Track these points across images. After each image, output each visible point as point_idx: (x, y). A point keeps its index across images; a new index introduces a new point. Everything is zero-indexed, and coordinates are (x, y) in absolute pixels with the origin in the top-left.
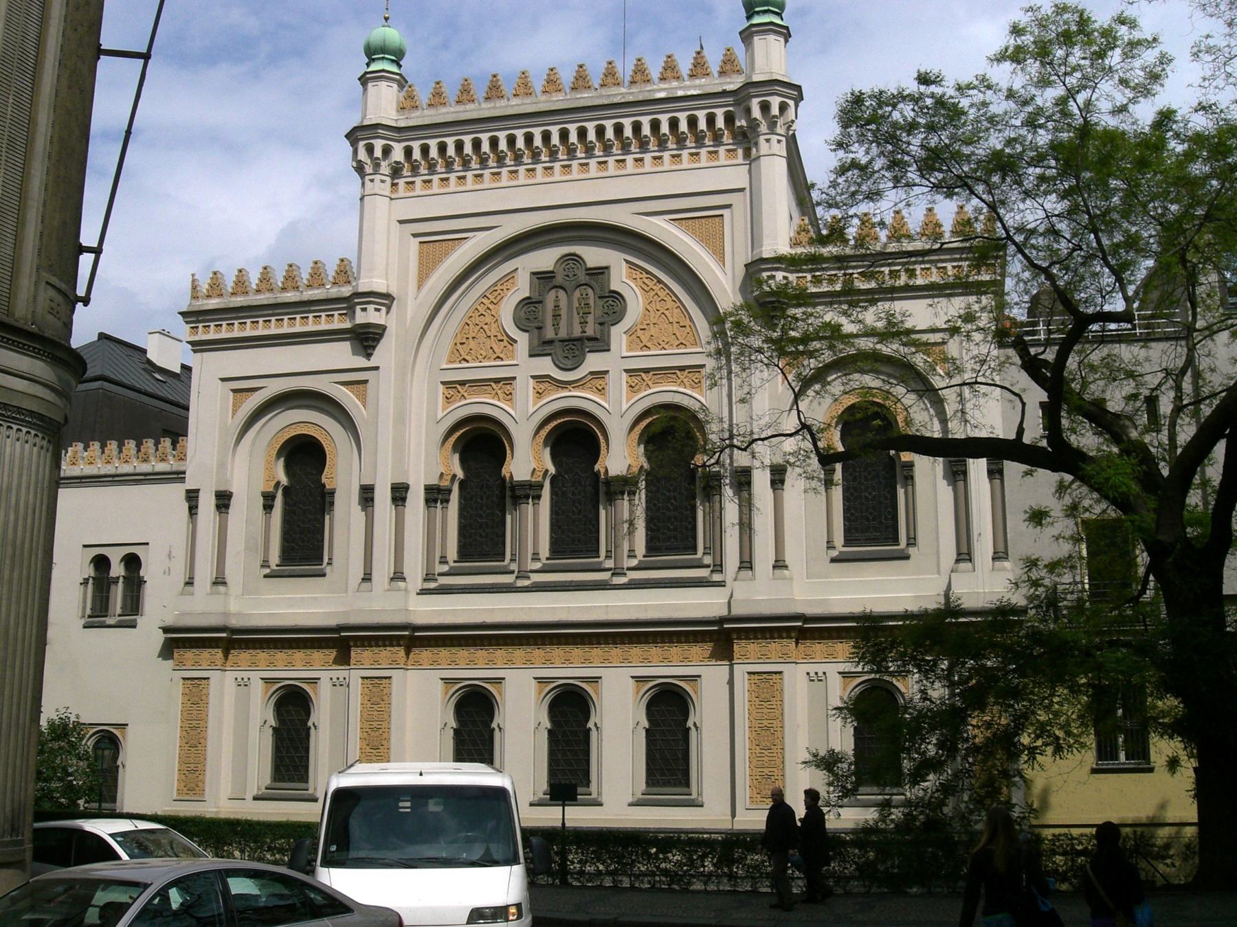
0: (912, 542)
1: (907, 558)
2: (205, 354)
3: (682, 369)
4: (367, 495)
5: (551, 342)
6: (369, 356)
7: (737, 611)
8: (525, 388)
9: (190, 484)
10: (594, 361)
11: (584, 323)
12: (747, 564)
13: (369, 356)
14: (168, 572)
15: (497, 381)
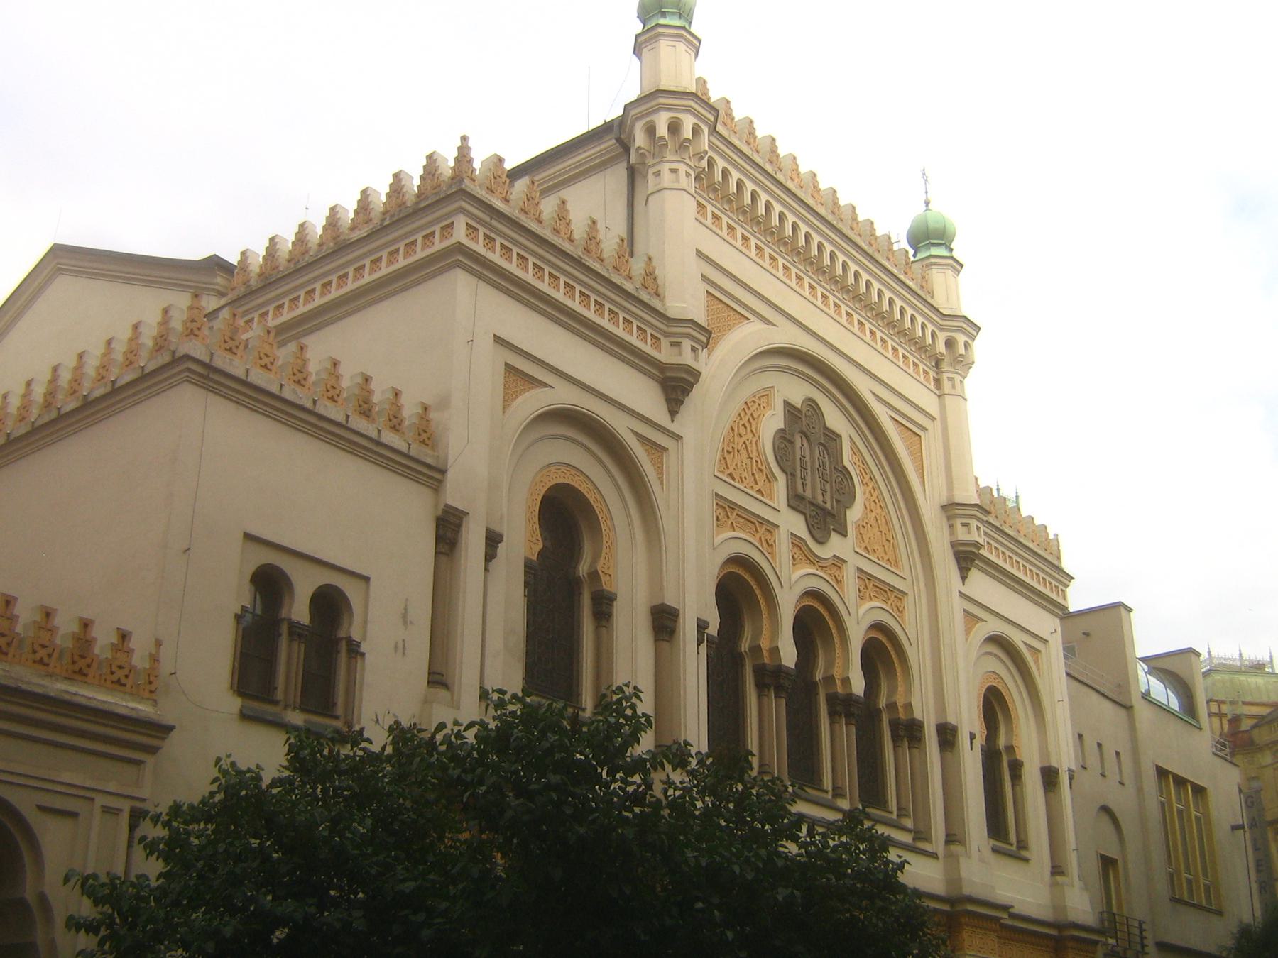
0: (1022, 845)
1: (1026, 860)
2: (482, 284)
3: (893, 589)
4: (664, 621)
5: (801, 498)
6: (673, 413)
7: (967, 891)
8: (784, 548)
9: (453, 497)
10: (836, 546)
11: (824, 491)
12: (952, 838)
13: (673, 413)
14: (401, 648)
15: (762, 521)
